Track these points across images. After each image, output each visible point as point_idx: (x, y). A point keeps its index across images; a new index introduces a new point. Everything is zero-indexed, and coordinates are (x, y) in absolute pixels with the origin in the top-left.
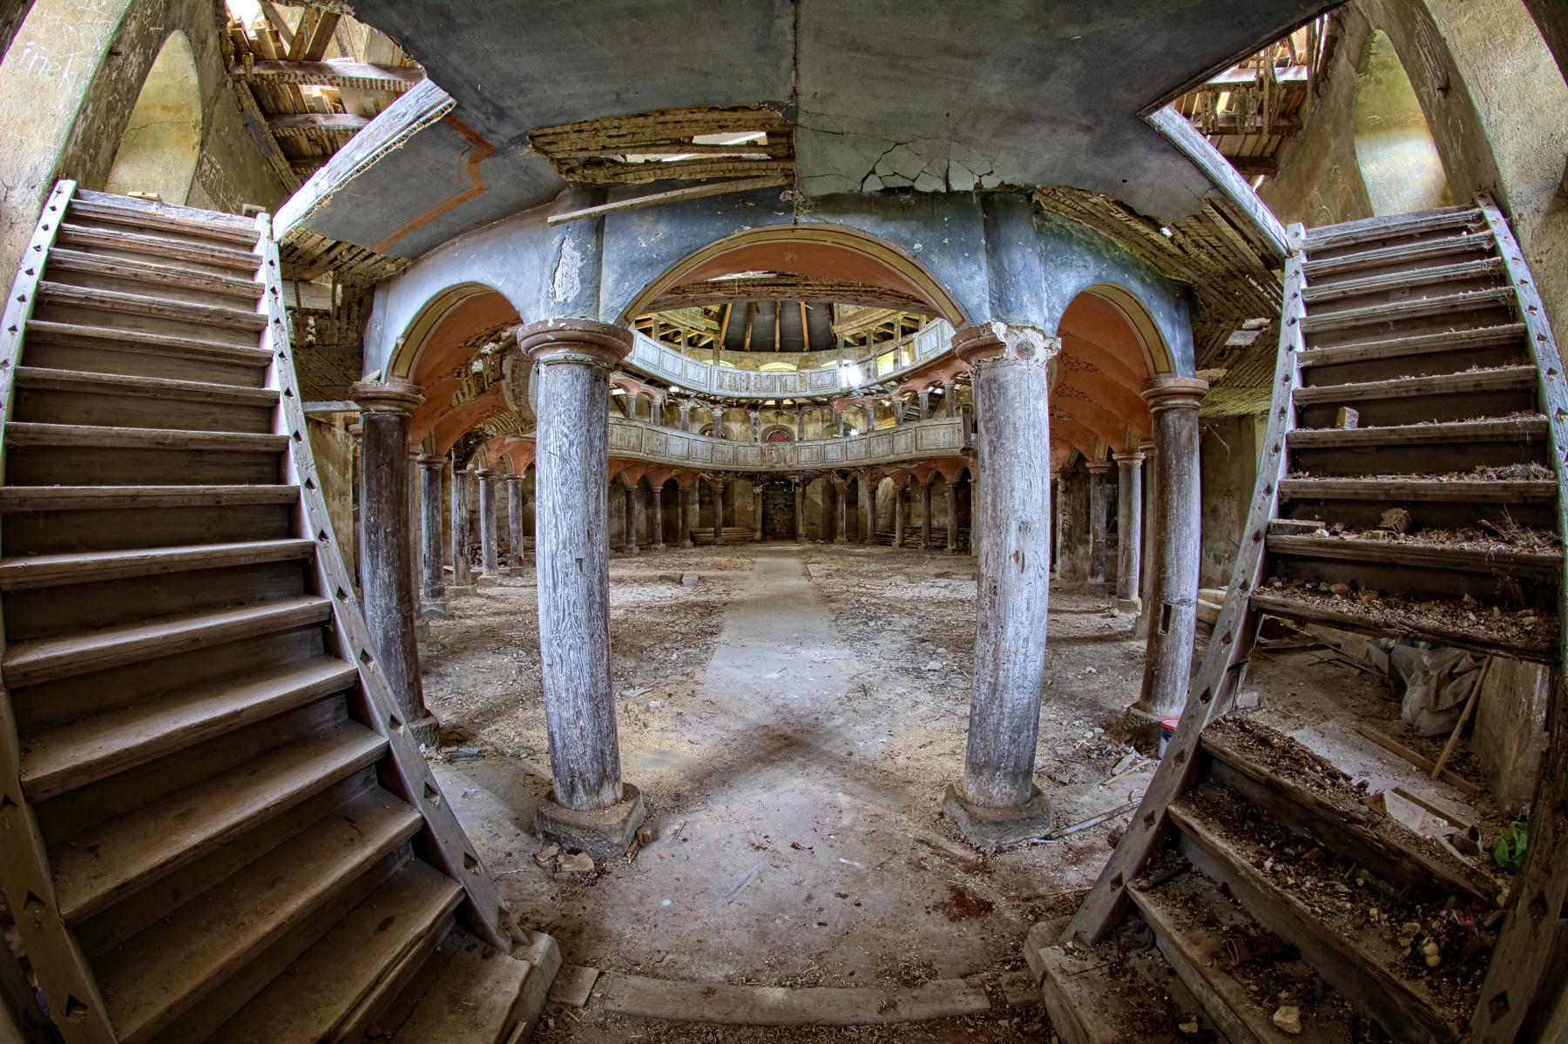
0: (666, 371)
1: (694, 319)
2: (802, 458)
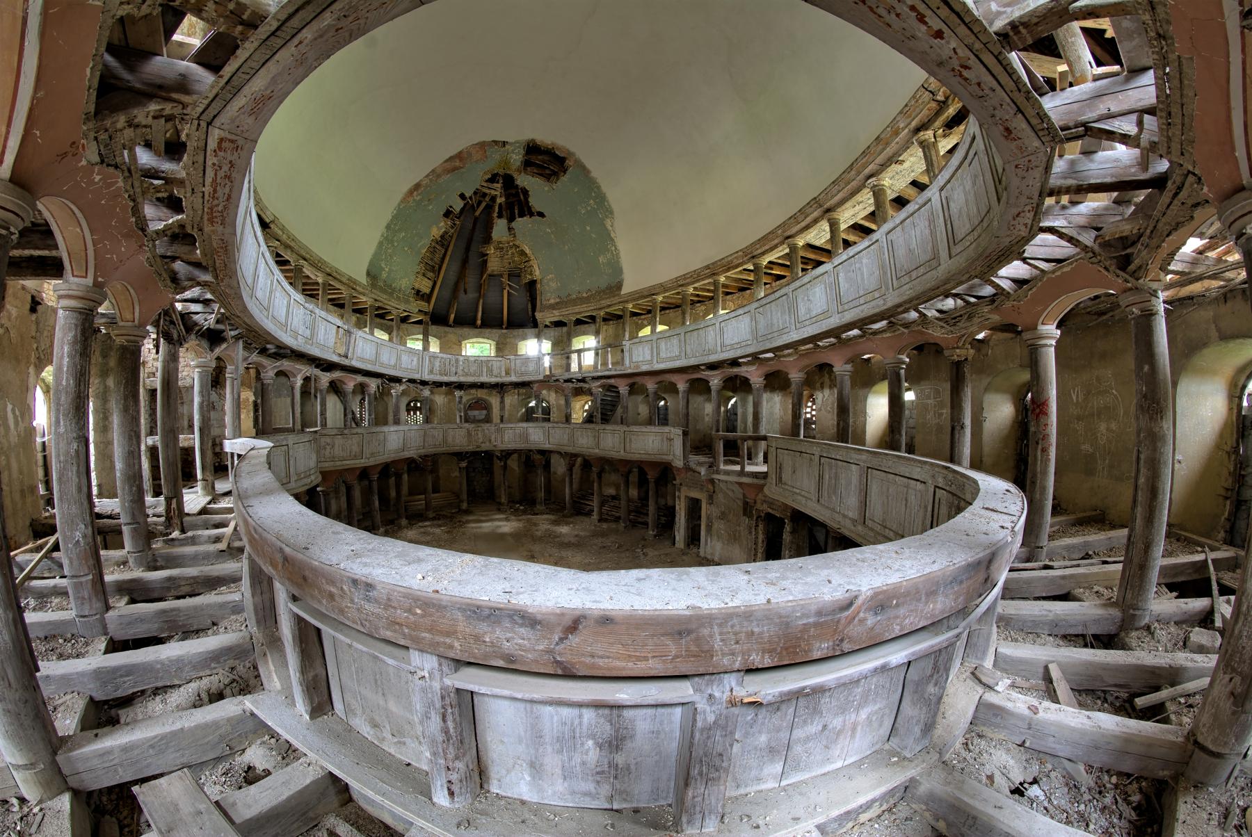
0: (382, 365)
1: (407, 302)
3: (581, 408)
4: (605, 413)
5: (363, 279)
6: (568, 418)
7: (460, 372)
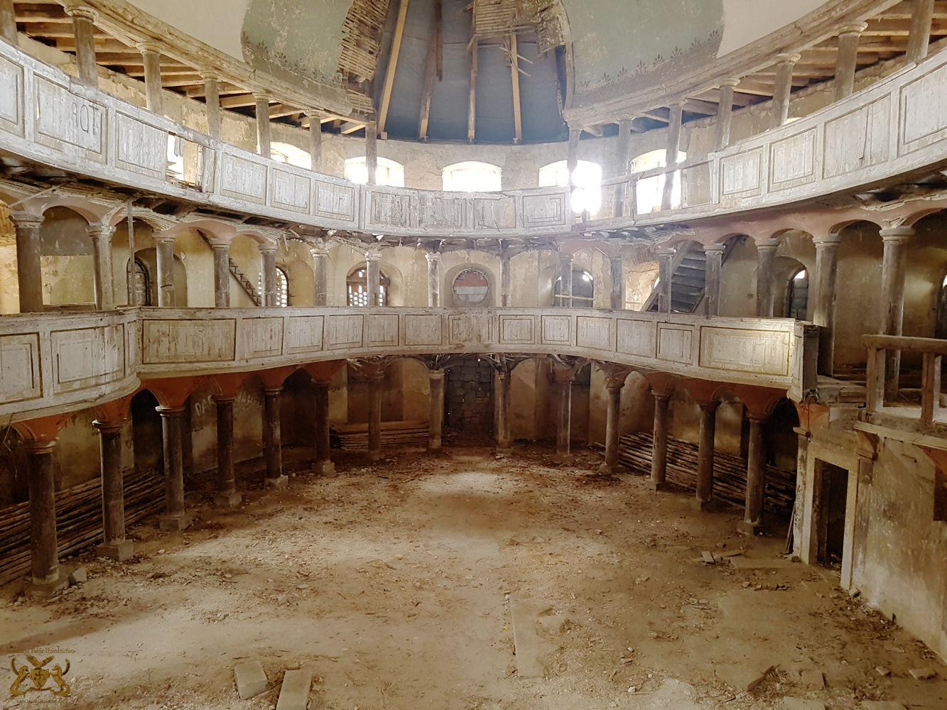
0: (278, 204)
1: (330, 95)
2: (507, 335)
3: (640, 288)
4: (686, 295)
5: (236, 50)
6: (617, 300)
7: (427, 216)
